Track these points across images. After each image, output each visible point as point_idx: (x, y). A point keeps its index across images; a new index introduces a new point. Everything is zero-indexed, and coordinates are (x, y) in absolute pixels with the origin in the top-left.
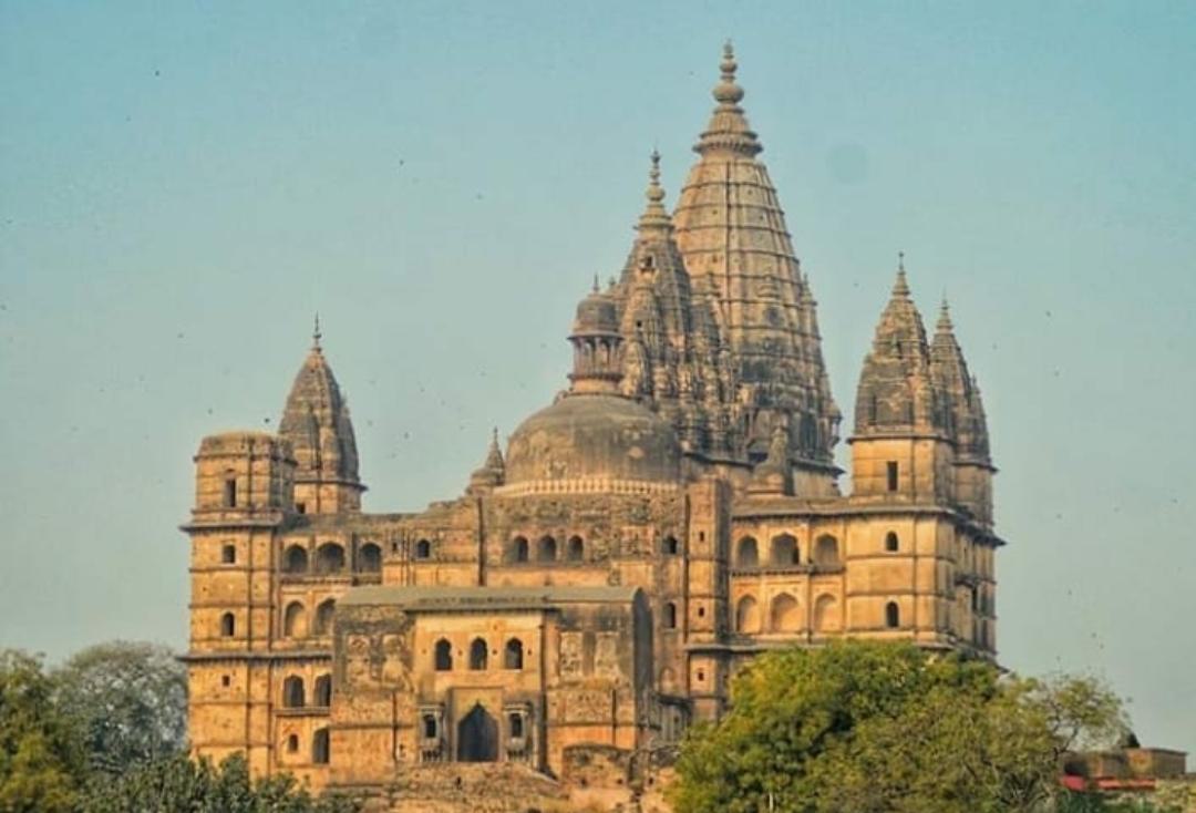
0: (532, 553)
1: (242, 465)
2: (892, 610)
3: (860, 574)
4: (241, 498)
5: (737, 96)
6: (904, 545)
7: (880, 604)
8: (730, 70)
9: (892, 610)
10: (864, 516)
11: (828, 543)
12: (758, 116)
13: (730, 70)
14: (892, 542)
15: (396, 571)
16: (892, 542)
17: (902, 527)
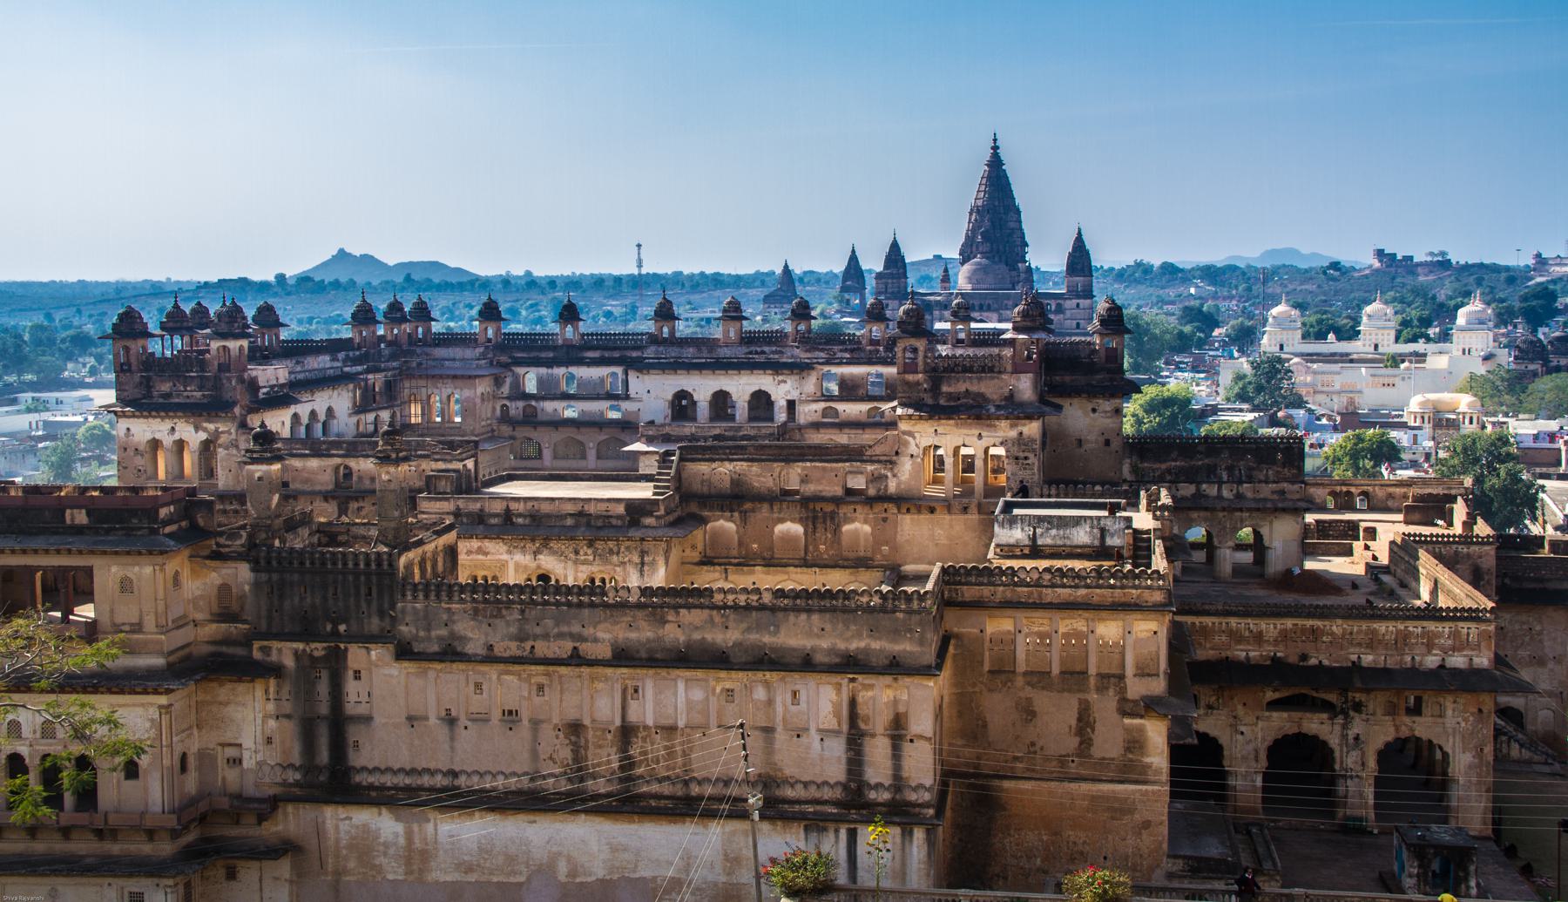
0: (977, 308)
1: (890, 281)
2: (1078, 324)
3: (1068, 313)
4: (890, 290)
5: (998, 148)
6: (1081, 306)
7: (1075, 322)
8: (995, 140)
9: (1078, 324)
10: (1070, 299)
11: (1059, 306)
12: (1002, 153)
13: (995, 140)
14: (1078, 305)
15: (937, 312)
16: (1078, 305)
17: (1081, 301)
